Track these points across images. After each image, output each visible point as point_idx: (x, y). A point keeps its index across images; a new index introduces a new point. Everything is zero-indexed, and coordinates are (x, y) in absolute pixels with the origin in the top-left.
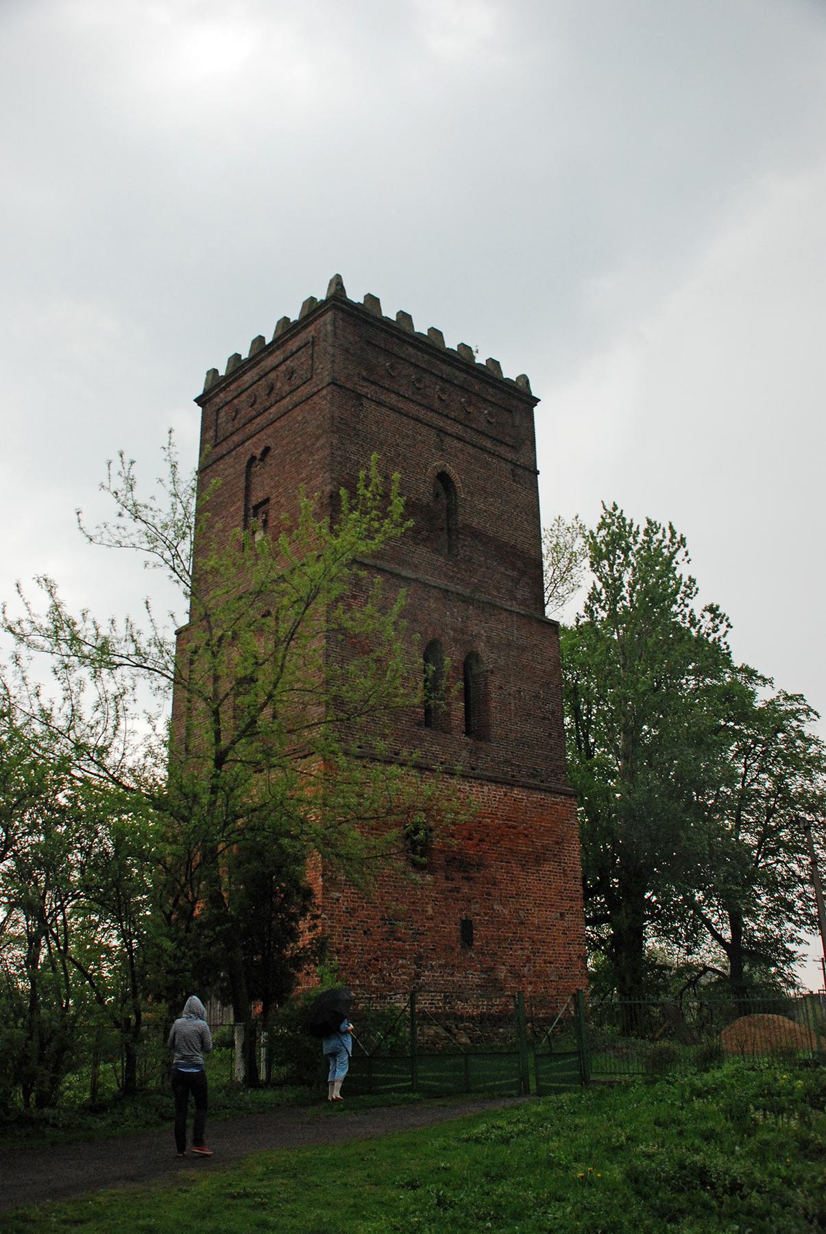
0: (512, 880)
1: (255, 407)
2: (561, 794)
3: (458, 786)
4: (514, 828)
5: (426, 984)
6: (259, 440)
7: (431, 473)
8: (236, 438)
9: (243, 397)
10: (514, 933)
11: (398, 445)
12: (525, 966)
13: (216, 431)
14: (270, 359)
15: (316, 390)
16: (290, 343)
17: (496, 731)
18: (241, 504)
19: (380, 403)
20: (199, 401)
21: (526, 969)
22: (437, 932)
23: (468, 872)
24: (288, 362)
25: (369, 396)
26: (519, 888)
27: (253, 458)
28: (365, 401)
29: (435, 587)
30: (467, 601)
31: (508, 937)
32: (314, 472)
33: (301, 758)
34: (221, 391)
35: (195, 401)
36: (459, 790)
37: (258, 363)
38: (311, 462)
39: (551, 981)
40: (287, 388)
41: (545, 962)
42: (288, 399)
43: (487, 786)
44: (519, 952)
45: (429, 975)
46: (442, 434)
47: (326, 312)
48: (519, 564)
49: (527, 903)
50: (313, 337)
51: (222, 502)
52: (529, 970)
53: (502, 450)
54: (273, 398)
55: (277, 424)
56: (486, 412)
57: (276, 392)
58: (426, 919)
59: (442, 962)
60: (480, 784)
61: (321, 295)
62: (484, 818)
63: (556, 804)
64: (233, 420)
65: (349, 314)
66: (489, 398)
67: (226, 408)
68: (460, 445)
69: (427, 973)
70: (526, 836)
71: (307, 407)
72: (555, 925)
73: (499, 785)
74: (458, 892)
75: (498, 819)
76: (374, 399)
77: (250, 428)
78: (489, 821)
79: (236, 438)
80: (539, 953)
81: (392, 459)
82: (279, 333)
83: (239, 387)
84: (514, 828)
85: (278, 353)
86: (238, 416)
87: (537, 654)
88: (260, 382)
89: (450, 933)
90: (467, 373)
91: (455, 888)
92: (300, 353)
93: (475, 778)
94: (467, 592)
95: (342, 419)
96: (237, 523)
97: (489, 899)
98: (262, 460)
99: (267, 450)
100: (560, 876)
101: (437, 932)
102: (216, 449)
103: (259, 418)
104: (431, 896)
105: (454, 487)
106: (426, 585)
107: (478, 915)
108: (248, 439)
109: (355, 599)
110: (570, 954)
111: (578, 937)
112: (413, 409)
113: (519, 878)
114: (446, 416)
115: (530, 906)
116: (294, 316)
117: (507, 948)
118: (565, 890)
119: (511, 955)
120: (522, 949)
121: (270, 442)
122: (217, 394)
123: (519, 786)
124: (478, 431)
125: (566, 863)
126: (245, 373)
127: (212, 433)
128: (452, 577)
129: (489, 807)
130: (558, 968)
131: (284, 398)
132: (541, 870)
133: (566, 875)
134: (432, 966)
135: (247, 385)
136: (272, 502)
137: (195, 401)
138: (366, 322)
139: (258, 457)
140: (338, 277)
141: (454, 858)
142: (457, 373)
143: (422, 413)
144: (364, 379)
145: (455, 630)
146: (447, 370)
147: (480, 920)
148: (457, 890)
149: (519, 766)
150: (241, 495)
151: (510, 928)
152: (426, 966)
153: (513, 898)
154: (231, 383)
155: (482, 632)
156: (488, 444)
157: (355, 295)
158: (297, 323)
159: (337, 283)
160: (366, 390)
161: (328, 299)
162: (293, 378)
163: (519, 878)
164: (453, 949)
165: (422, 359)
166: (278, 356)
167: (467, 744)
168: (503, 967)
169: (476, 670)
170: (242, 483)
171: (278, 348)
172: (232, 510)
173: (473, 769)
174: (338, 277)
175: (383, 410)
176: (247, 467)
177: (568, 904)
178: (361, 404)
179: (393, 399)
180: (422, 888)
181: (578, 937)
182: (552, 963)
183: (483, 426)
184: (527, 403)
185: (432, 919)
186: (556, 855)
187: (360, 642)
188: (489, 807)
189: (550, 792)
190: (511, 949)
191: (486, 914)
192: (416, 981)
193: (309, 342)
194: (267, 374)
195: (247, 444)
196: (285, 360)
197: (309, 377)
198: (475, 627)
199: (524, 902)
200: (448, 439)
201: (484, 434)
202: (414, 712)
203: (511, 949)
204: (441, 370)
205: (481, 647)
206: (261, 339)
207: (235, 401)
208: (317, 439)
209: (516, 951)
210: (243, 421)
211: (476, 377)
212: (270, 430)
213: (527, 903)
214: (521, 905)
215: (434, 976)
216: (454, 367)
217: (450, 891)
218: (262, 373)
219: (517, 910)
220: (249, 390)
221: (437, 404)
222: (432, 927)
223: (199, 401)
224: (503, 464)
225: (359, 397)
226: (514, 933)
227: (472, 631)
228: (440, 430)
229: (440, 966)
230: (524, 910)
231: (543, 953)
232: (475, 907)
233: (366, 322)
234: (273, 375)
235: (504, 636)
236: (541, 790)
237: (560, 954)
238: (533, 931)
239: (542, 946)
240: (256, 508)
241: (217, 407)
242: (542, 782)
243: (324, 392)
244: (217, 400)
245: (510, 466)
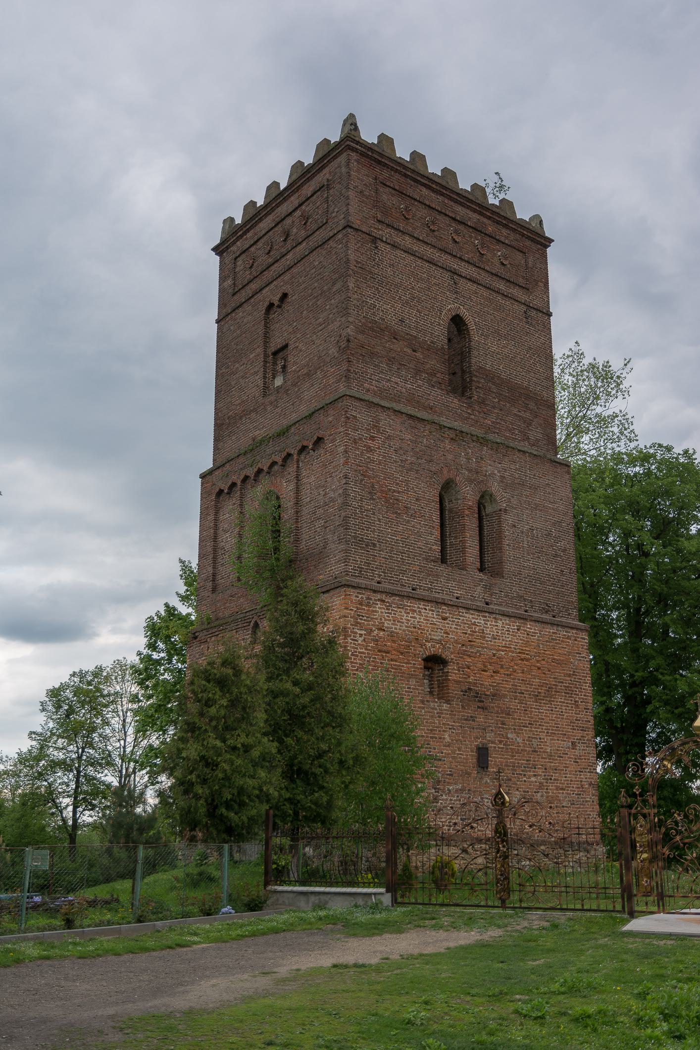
0: (526, 710)
1: (272, 253)
2: (572, 628)
3: (473, 621)
4: (527, 660)
5: (444, 807)
6: (276, 286)
7: (446, 317)
8: (254, 286)
9: (260, 244)
10: (527, 761)
11: (413, 288)
12: (538, 792)
13: (234, 279)
14: (285, 204)
15: (331, 234)
16: (305, 187)
17: (509, 567)
18: (260, 350)
19: (395, 246)
20: (215, 249)
21: (539, 795)
22: (454, 758)
23: (483, 702)
24: (303, 207)
25: (384, 239)
26: (532, 718)
27: (271, 305)
28: (381, 245)
29: (450, 428)
30: (483, 442)
31: (522, 764)
32: (331, 316)
33: (323, 593)
35: (213, 249)
36: (474, 624)
37: (273, 210)
38: (328, 307)
39: (563, 807)
40: (303, 233)
41: (557, 788)
42: (304, 244)
43: (501, 620)
44: (533, 779)
45: (447, 799)
46: (455, 277)
47: (340, 153)
48: (532, 405)
49: (540, 732)
50: (328, 180)
51: (242, 350)
52: (542, 796)
53: (515, 292)
55: (295, 270)
56: (499, 253)
57: (292, 238)
58: (445, 746)
59: (460, 786)
60: (495, 618)
61: (335, 137)
62: (498, 650)
63: (569, 638)
64: (251, 267)
65: (363, 154)
66: (502, 239)
67: (244, 256)
68: (474, 287)
69: (444, 797)
70: (539, 668)
71: (324, 252)
72: (567, 754)
73: (513, 619)
74: (474, 721)
75: (513, 652)
76: (388, 241)
78: (503, 653)
79: (254, 286)
80: (551, 779)
81: (407, 303)
82: (294, 177)
83: (256, 234)
84: (527, 660)
85: (292, 198)
86: (255, 264)
87: (549, 493)
88: (276, 229)
89: (467, 759)
90: (481, 214)
91: (471, 717)
92: (315, 197)
93: (489, 613)
94: (479, 432)
95: (357, 262)
96: (256, 370)
97: (503, 728)
98: (279, 306)
99: (285, 296)
100: (572, 707)
101: (454, 758)
102: (235, 297)
103: (276, 265)
104: (448, 725)
105: (467, 329)
106: (442, 427)
107: (493, 742)
108: (266, 286)
109: (373, 441)
110: (581, 781)
111: (589, 766)
112: (429, 252)
113: (531, 708)
114: (461, 259)
115: (543, 735)
116: (308, 160)
117: (521, 774)
118: (576, 720)
119: (525, 781)
120: (535, 775)
121: (287, 288)
122: (234, 243)
123: (531, 621)
124: (492, 274)
125: (578, 695)
126: (261, 220)
127: (229, 282)
128: (467, 418)
129: (503, 640)
130: (570, 794)
131: (300, 243)
132: (554, 701)
133: (577, 706)
134: (449, 790)
135: (263, 232)
136: (290, 347)
137: (213, 249)
138: (379, 162)
139: (276, 303)
140: (352, 116)
141: (469, 689)
142: (471, 214)
143: (436, 255)
144: (379, 221)
145: (470, 471)
146: (461, 212)
147: (495, 747)
148: (473, 719)
149: (531, 601)
150: (260, 341)
151: (524, 756)
152: (443, 791)
153: (527, 727)
154: (248, 231)
155: (496, 472)
156: (502, 286)
157: (369, 136)
158: (311, 166)
159: (351, 123)
160: (380, 232)
161: (342, 140)
162: (308, 224)
163: (531, 708)
164: (469, 774)
165: (436, 200)
166: (294, 200)
167: (481, 580)
168: (517, 793)
169: (489, 509)
170: (261, 330)
171: (294, 192)
172: (251, 356)
173: (487, 604)
174: (352, 116)
175: (398, 252)
176: (265, 314)
177: (579, 734)
178: (376, 248)
179: (407, 242)
180: (440, 717)
181: (589, 766)
182: (564, 790)
183: (497, 269)
184: (541, 244)
185: (449, 746)
186: (568, 687)
187: (378, 482)
188: (503, 640)
189: (562, 626)
190: (525, 775)
191: (500, 742)
192: (435, 804)
193: (323, 186)
194: (283, 220)
195: (264, 291)
196: (300, 205)
197: (325, 221)
198: (490, 467)
199: (537, 731)
200: (462, 281)
201: (497, 275)
202: (430, 549)
203: (525, 775)
204: (454, 212)
205: (495, 487)
206: (275, 184)
207: (252, 249)
208: (334, 284)
209: (529, 778)
210: (260, 269)
211: (489, 218)
212: (287, 277)
213: (540, 732)
214: (534, 734)
215: (451, 800)
216: (468, 207)
217: (466, 720)
218: (278, 220)
219: (530, 739)
221: (451, 245)
222: (449, 754)
223: (215, 249)
224: (516, 306)
225: (375, 240)
226: (527, 761)
227: (486, 471)
228: (454, 272)
229: (457, 791)
230: (537, 739)
231: (555, 780)
232: (490, 736)
233: (379, 162)
234: (288, 221)
235: (517, 476)
236: (552, 624)
237: (571, 781)
238: (545, 758)
239: (554, 773)
240: (275, 354)
241: (234, 256)
242: (554, 617)
243: (340, 236)
244: (234, 248)
245: (524, 308)
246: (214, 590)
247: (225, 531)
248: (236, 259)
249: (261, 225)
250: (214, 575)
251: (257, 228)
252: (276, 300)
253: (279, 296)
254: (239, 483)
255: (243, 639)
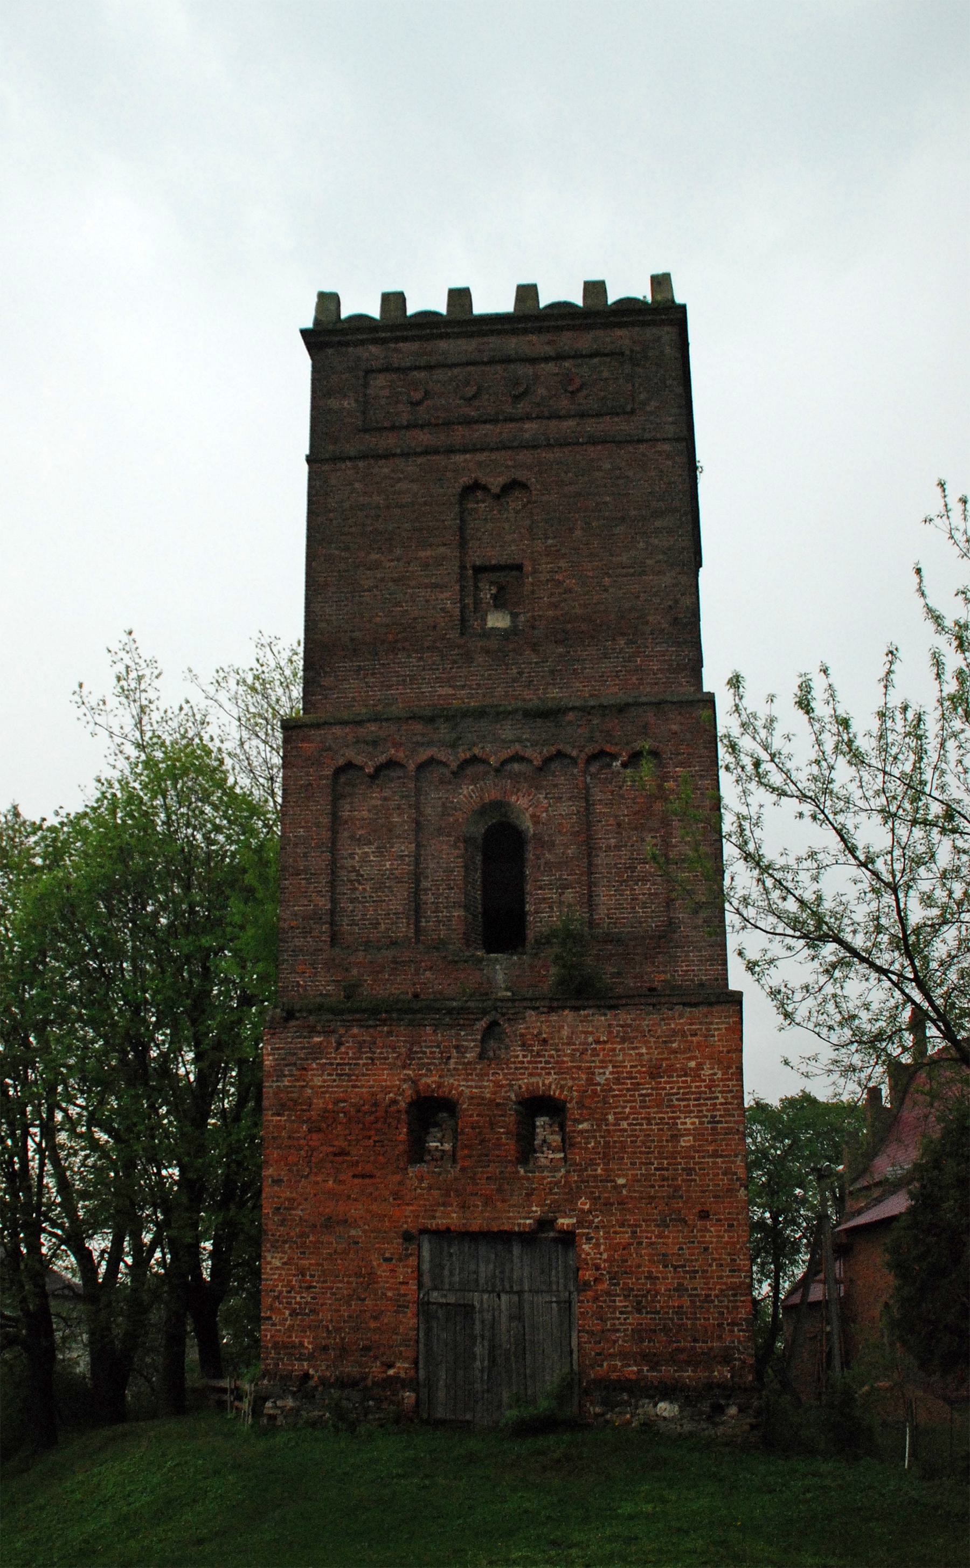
8: (424, 438)
27: (475, 487)
34: (375, 341)
38: (641, 545)
42: (571, 423)
54: (522, 407)
77: (460, 434)
99: (513, 486)
121: (521, 475)
154: (405, 339)
172: (422, 554)
195: (459, 458)
208: (658, 514)
220: (456, 371)
244: (360, 351)
246: (334, 939)
247: (359, 841)
248: (368, 372)
249: (443, 345)
250: (332, 912)
251: (429, 346)
252: (496, 483)
253: (501, 480)
254: (412, 766)
255: (457, 1047)
